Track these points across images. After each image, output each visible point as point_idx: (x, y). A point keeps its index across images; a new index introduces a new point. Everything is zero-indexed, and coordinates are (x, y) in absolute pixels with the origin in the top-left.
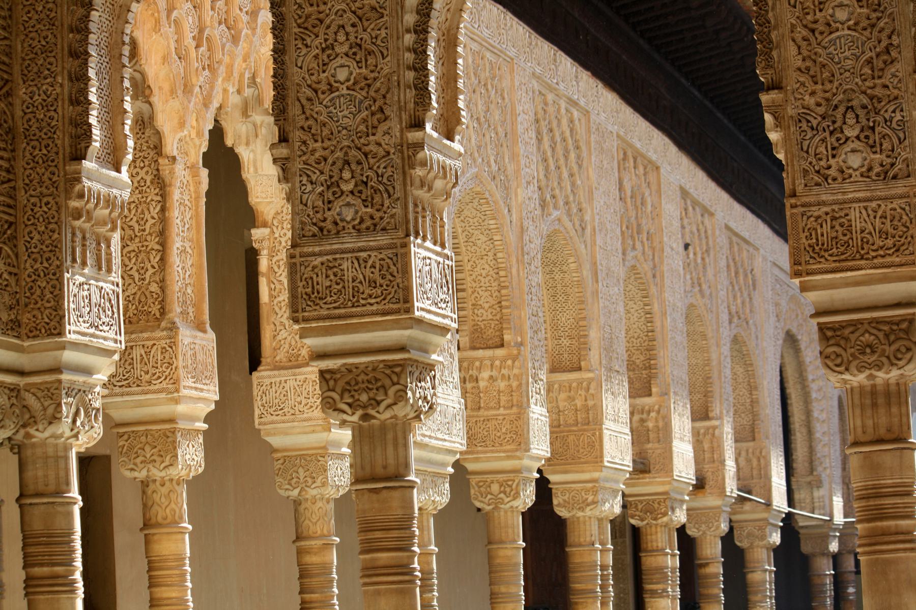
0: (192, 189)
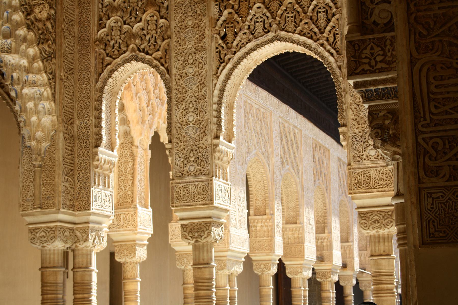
0: (145, 157)
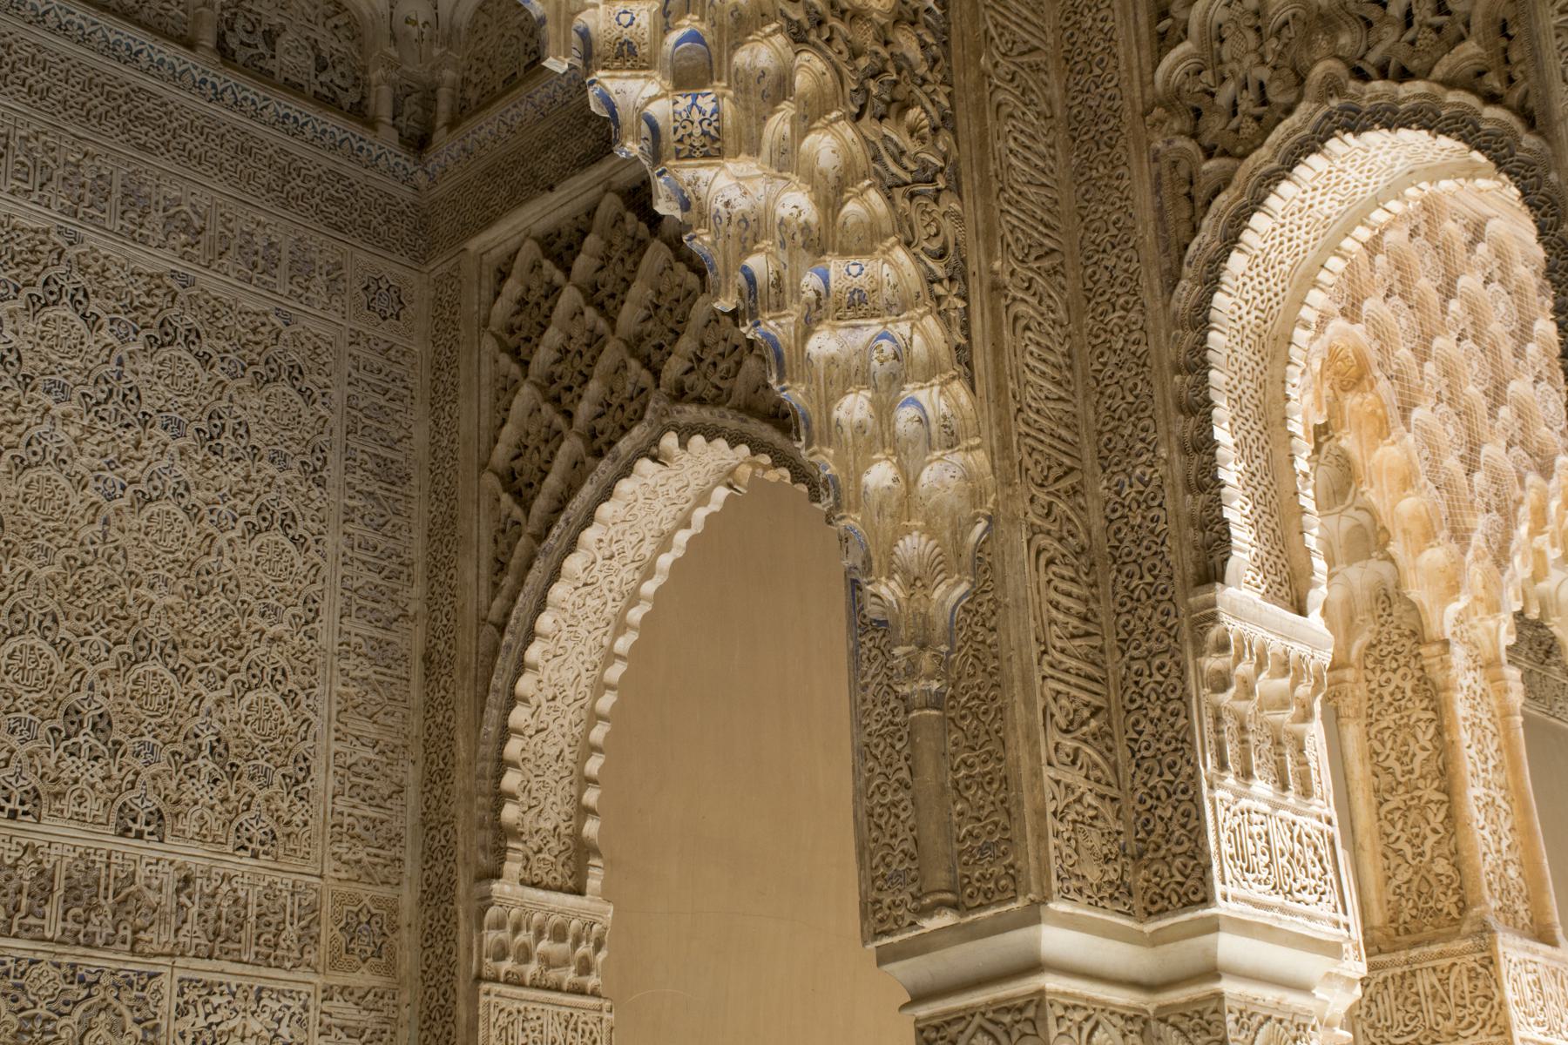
0: (1494, 702)
